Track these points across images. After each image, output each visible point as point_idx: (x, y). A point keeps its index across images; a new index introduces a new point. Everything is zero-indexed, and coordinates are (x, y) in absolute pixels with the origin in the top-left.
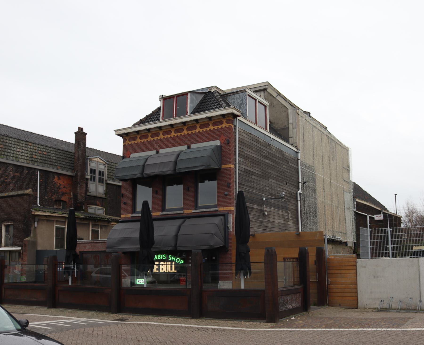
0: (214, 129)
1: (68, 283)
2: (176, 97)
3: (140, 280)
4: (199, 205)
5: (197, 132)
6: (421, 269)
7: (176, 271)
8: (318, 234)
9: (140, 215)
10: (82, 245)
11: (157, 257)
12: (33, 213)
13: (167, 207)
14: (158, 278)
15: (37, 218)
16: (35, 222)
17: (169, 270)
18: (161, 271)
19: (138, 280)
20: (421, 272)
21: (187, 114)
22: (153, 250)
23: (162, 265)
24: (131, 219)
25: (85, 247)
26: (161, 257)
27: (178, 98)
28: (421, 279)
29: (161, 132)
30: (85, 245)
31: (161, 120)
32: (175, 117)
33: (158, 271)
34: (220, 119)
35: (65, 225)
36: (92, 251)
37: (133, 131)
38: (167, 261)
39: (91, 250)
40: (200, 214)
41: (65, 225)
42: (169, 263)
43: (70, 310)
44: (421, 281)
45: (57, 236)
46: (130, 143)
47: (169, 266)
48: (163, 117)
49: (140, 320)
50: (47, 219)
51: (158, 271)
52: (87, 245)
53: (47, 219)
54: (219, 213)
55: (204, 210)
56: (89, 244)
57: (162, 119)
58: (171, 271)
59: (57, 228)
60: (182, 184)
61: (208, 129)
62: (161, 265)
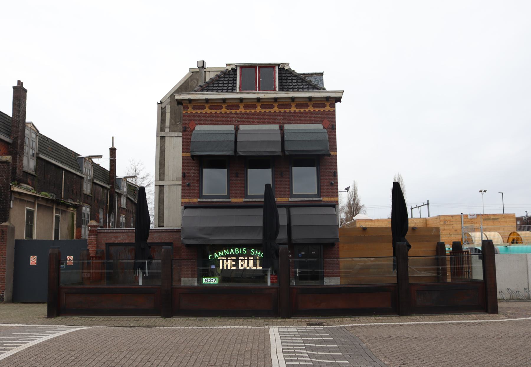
0: (314, 111)
1: (138, 282)
2: (259, 67)
3: (209, 278)
4: (294, 193)
5: (258, 112)
6: (529, 263)
7: (261, 268)
8: (434, 230)
9: (263, 200)
10: (111, 235)
11: (234, 251)
12: (12, 189)
13: (204, 193)
14: (227, 277)
15: (13, 196)
16: (11, 200)
17: (251, 266)
18: (240, 268)
19: (206, 278)
20: (529, 265)
21: (275, 90)
22: (277, 242)
23: (242, 260)
24: (198, 205)
25: (116, 237)
26: (239, 250)
27: (261, 69)
28: (529, 272)
29: (224, 106)
30: (116, 235)
31: (238, 90)
32: (259, 90)
33: (235, 268)
34: (321, 101)
35: (34, 207)
36: (117, 243)
37: (187, 98)
38: (248, 255)
39: (127, 242)
40: (308, 203)
41: (34, 207)
42: (252, 258)
43: (209, 319)
44: (529, 274)
45: (27, 222)
46: (194, 112)
47: (251, 262)
48: (240, 87)
49: (352, 322)
50: (20, 198)
51: (235, 268)
52: (119, 234)
53: (20, 198)
54: (322, 203)
55: (305, 199)
56: (124, 234)
57: (240, 90)
58: (255, 268)
59: (28, 211)
60: (270, 168)
61: (307, 110)
62: (240, 261)
